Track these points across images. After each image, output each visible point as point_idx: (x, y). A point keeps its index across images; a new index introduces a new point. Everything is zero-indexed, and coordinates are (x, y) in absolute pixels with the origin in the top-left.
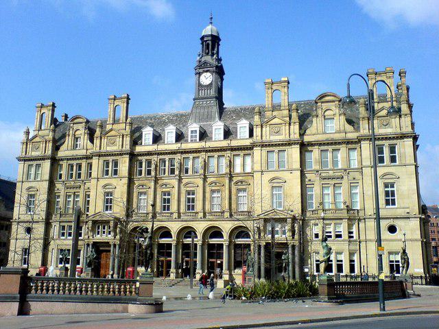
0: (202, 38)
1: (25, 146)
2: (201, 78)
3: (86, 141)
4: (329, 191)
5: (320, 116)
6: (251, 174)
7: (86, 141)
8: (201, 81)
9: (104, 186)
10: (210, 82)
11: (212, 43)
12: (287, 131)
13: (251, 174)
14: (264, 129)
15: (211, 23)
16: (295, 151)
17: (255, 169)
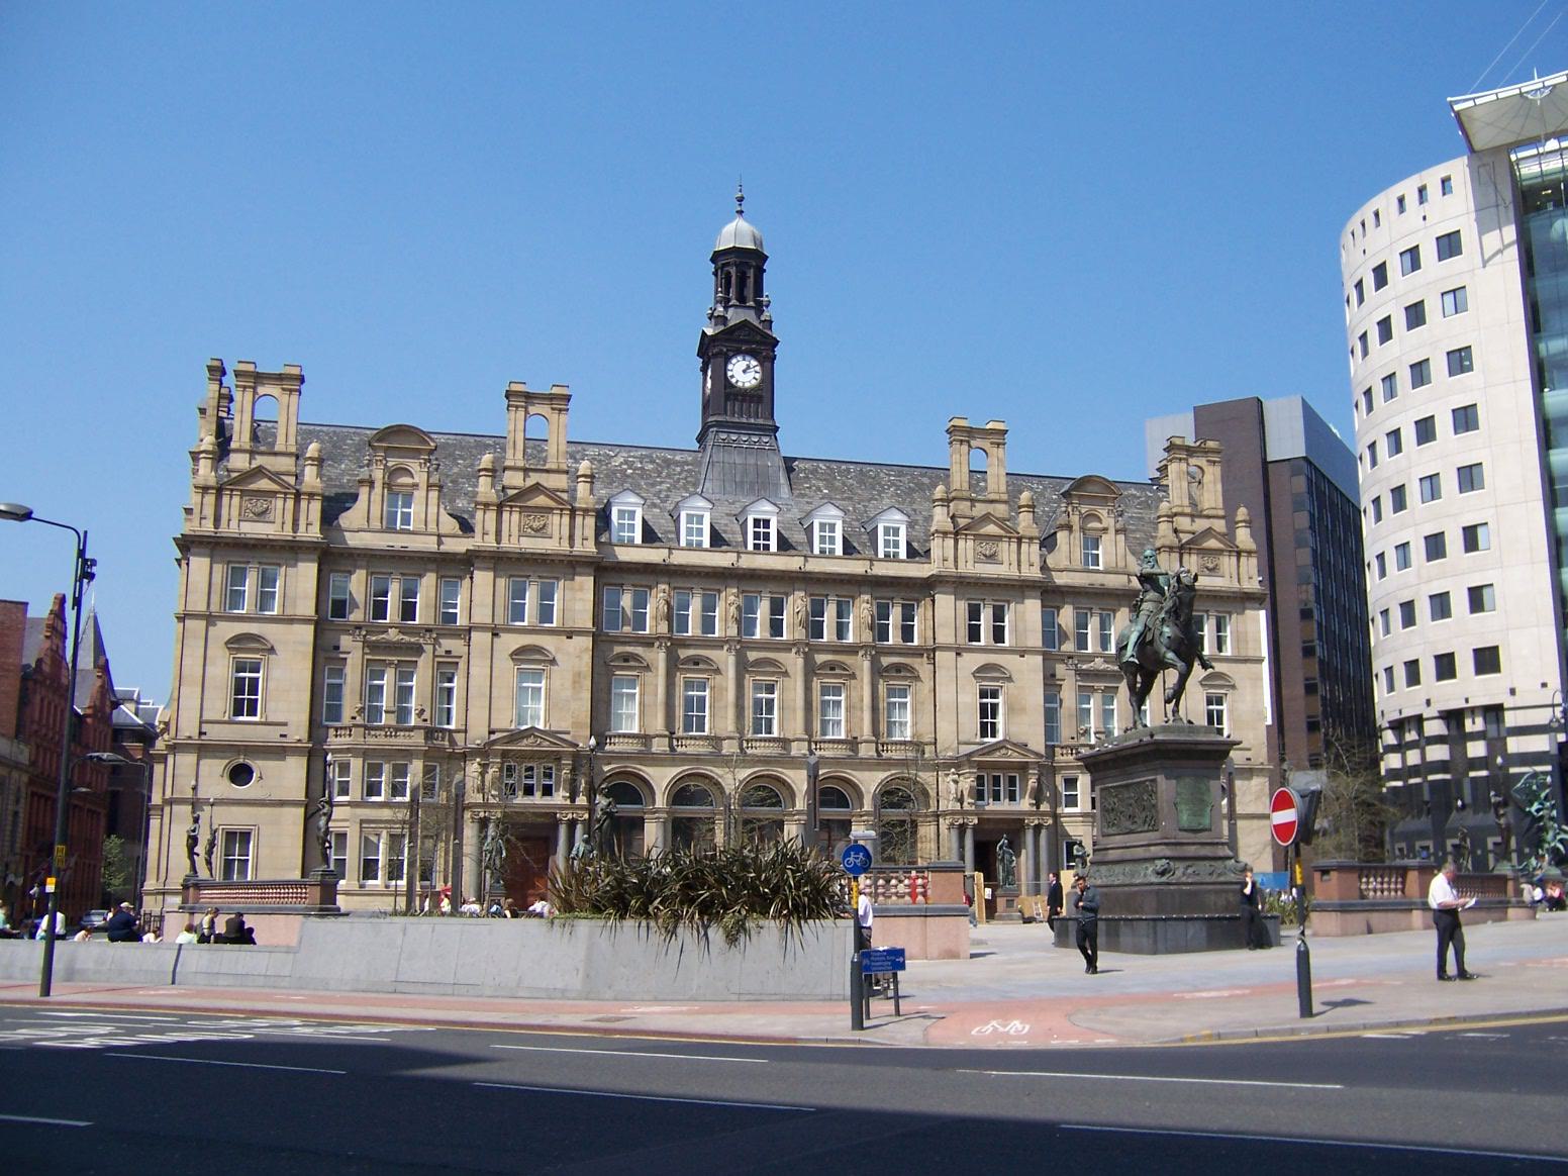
0: (716, 257)
1: (210, 499)
2: (730, 367)
3: (433, 509)
4: (1094, 704)
5: (1076, 527)
6: (930, 652)
7: (433, 509)
8: (729, 374)
9: (519, 654)
10: (754, 382)
11: (740, 272)
12: (1014, 556)
13: (930, 652)
14: (961, 543)
15: (740, 212)
16: (1032, 608)
17: (940, 640)
